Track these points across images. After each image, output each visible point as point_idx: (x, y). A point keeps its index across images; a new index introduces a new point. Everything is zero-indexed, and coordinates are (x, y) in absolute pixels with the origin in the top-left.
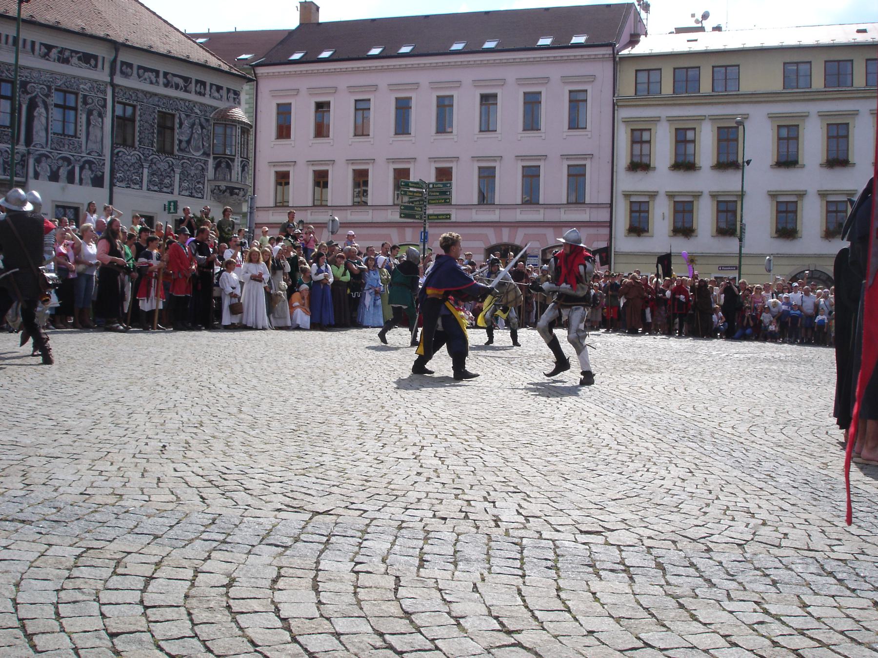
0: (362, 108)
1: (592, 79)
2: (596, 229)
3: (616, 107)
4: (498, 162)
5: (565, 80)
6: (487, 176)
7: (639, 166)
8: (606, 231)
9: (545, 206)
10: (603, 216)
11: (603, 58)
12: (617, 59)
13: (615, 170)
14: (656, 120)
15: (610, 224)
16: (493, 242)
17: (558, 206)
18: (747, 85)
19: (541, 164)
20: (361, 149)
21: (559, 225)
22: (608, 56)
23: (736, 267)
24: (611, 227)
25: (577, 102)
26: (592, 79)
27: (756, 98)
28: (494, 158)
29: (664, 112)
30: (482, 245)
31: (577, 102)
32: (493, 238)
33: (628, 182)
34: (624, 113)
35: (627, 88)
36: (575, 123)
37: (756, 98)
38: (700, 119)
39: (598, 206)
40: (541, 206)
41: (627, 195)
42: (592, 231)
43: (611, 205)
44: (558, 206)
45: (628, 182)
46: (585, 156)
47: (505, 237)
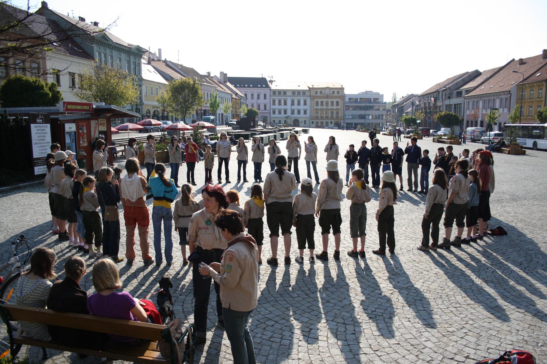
10: (269, 112)
15: (270, 113)
35: (272, 94)
36: (265, 98)
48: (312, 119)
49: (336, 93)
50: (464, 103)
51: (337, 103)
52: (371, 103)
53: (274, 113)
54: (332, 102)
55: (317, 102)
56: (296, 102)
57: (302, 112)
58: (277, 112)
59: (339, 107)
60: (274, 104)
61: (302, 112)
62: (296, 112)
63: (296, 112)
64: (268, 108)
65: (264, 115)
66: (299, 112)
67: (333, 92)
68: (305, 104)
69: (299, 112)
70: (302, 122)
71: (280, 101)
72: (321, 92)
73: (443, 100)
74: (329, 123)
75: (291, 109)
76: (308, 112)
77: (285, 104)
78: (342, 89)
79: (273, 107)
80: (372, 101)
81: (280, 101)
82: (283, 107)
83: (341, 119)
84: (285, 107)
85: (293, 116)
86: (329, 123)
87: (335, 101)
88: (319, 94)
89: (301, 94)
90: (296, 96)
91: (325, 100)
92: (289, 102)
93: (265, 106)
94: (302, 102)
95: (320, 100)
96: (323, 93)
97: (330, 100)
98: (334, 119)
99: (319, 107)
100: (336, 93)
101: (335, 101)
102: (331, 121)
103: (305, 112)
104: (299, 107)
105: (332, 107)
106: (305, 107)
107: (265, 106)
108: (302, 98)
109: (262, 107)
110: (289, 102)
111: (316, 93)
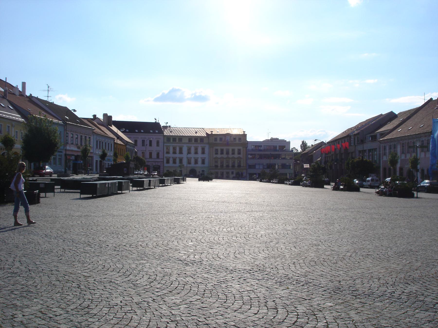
7: (168, 153)
8: (162, 163)
10: (162, 160)
14: (170, 146)
15: (163, 162)
18: (183, 141)
27: (185, 143)
29: (171, 145)
33: (166, 155)
34: (165, 144)
35: (165, 141)
37: (185, 143)
38: (177, 146)
39: (162, 159)
41: (166, 157)
45: (166, 155)
50: (380, 148)
51: (239, 150)
53: (168, 162)
54: (233, 150)
55: (217, 150)
57: (200, 161)
58: (171, 161)
59: (241, 156)
61: (200, 161)
64: (161, 156)
65: (157, 164)
66: (196, 162)
68: (203, 153)
69: (196, 162)
71: (174, 149)
72: (221, 139)
73: (355, 146)
75: (187, 158)
76: (206, 161)
77: (181, 152)
78: (245, 136)
80: (278, 148)
81: (174, 149)
84: (181, 156)
86: (231, 173)
89: (199, 141)
91: (225, 148)
92: (185, 150)
93: (158, 155)
94: (200, 151)
96: (223, 140)
97: (231, 148)
99: (219, 156)
101: (236, 148)
102: (232, 171)
103: (203, 162)
104: (196, 156)
107: (158, 155)
108: (199, 145)
110: (185, 150)
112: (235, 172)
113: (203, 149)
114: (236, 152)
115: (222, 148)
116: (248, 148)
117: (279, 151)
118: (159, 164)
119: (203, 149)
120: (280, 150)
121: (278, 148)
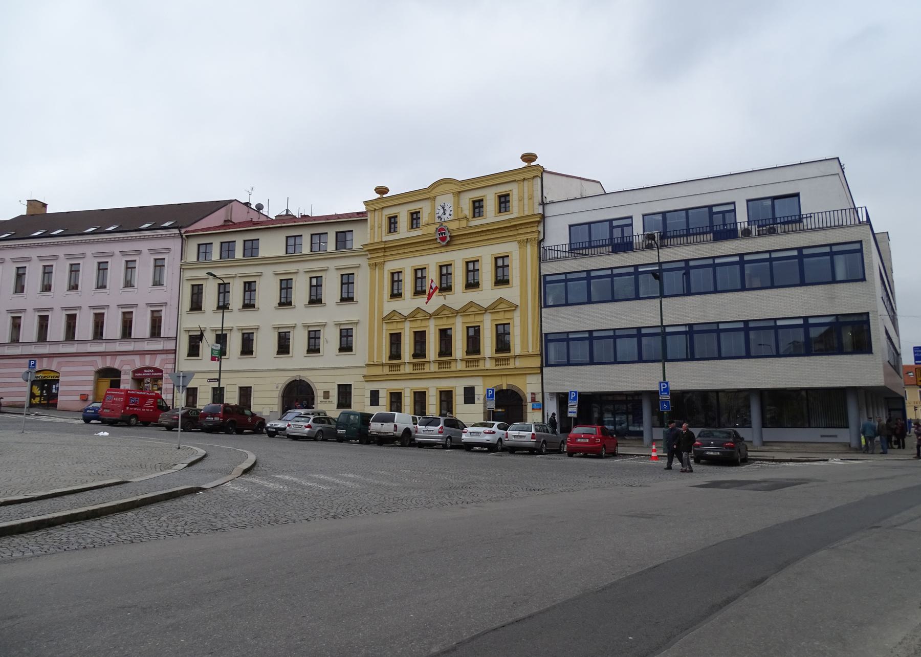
0: (102, 268)
1: (168, 251)
2: (166, 355)
3: (182, 270)
4: (106, 309)
5: (96, 255)
6: (71, 320)
8: (172, 356)
9: (50, 343)
10: (170, 345)
11: (174, 237)
12: (184, 237)
13: (179, 313)
15: (175, 352)
16: (100, 366)
17: (142, 340)
19: (163, 308)
20: (73, 299)
21: (142, 353)
22: (178, 235)
23: (217, 379)
24: (175, 353)
25: (159, 265)
26: (168, 251)
28: (103, 307)
30: (93, 369)
31: (159, 265)
32: (101, 363)
34: (189, 274)
35: (192, 256)
39: (168, 339)
40: (133, 340)
42: (164, 356)
43: (176, 337)
44: (142, 340)
46: (161, 305)
47: (108, 363)
48: (368, 378)
49: (490, 205)
52: (728, 233)
54: (472, 268)
55: (396, 278)
56: (300, 293)
57: (330, 340)
59: (511, 293)
60: (196, 306)
61: (330, 340)
62: (299, 342)
63: (299, 342)
65: (148, 361)
67: (478, 206)
70: (326, 395)
74: (459, 398)
76: (360, 340)
79: (193, 322)
80: (742, 217)
82: (237, 320)
83: (523, 373)
85: (284, 362)
87: (485, 254)
88: (404, 231)
90: (304, 259)
91: (431, 261)
92: (267, 293)
94: (331, 289)
95: (406, 265)
96: (424, 218)
97: (457, 258)
98: (486, 374)
100: (490, 205)
102: (469, 383)
105: (473, 296)
106: (347, 314)
108: (332, 264)
109: (141, 327)
111: (393, 222)
112: (481, 388)
113: (347, 281)
114: (487, 275)
115: (419, 262)
116: (547, 244)
117: (747, 233)
118: (157, 365)
119: (347, 281)
120: (754, 230)
121: (742, 217)
